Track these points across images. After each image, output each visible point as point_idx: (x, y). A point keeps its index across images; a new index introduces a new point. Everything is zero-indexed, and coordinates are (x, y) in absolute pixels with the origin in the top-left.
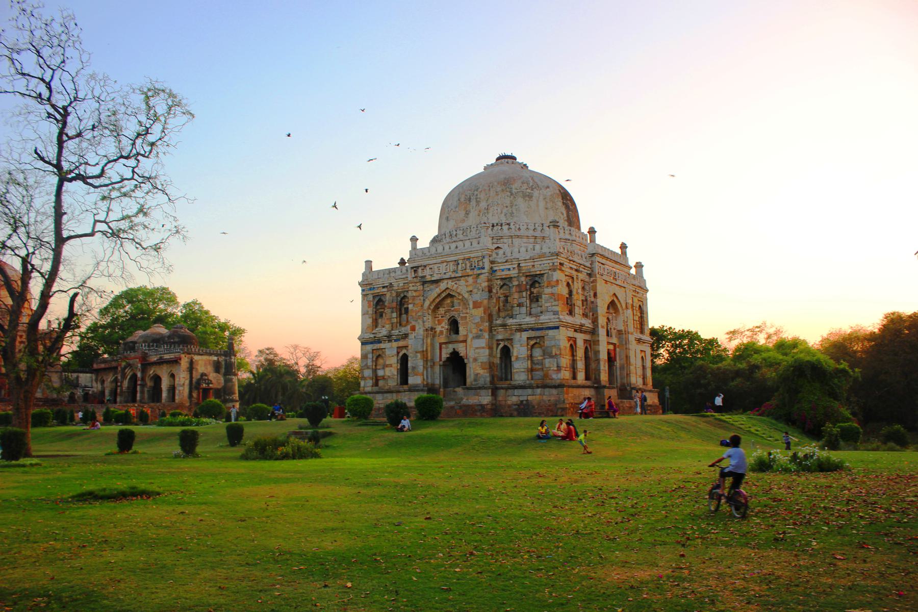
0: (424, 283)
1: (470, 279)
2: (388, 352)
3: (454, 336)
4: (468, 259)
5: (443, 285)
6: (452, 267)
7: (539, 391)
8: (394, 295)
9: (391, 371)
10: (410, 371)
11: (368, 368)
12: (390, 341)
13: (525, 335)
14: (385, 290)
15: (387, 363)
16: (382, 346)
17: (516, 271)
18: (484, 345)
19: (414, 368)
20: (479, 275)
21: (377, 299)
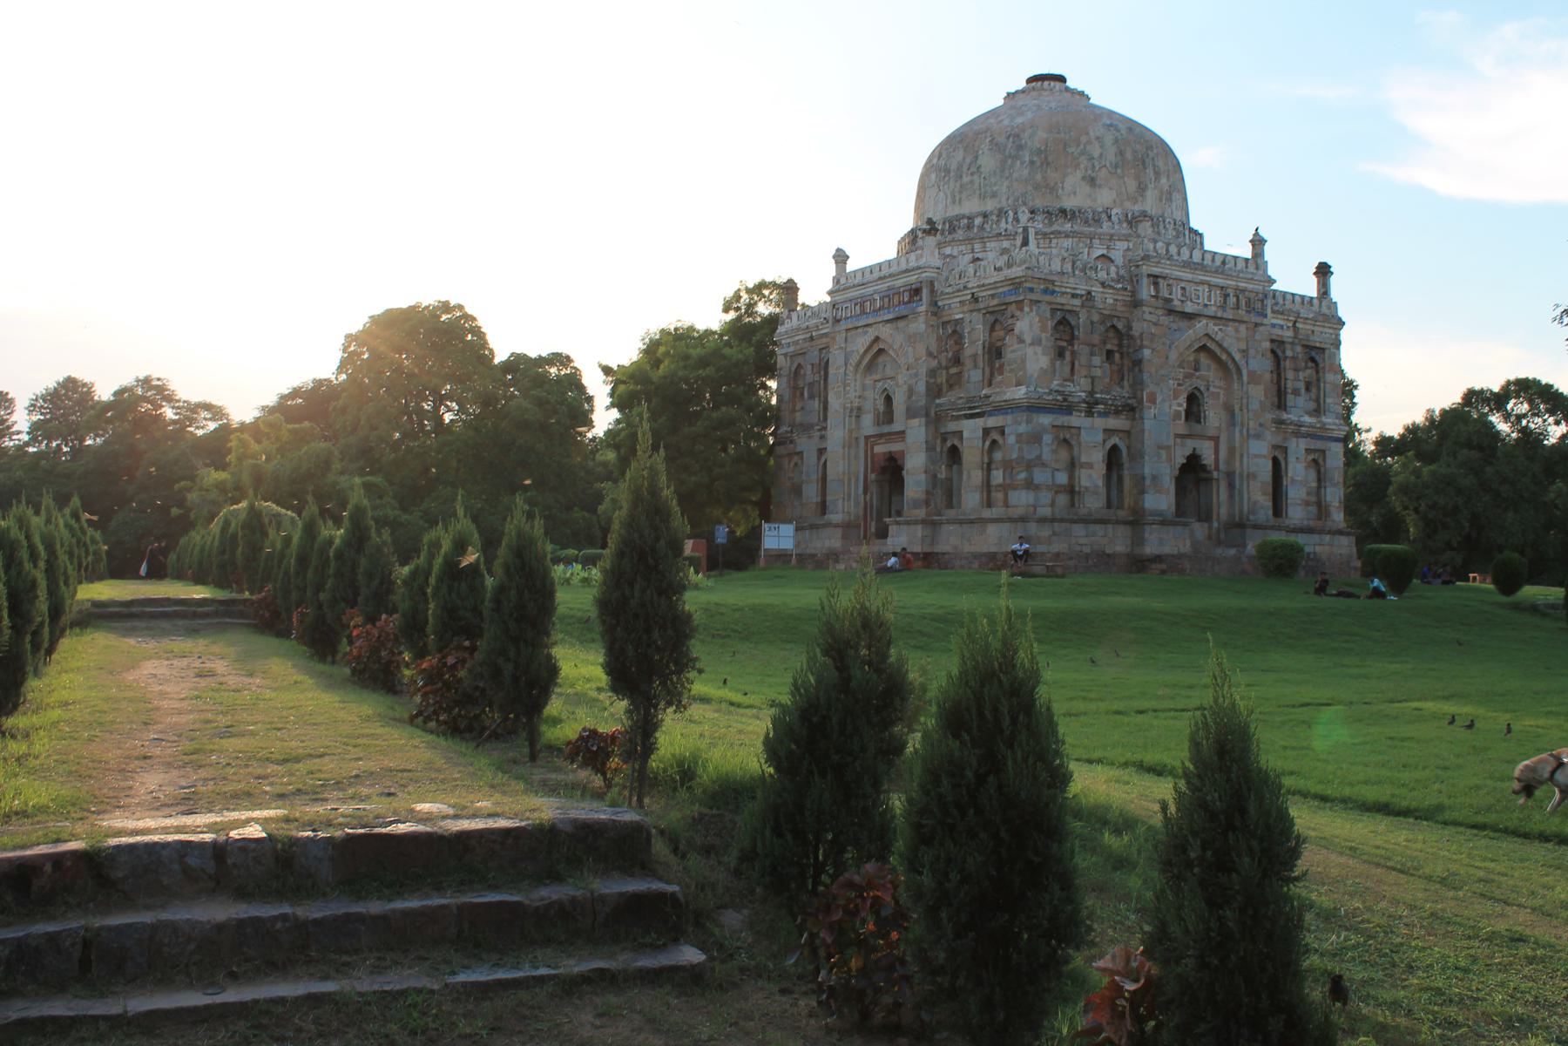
0: (1171, 312)
1: (1243, 328)
2: (1084, 436)
3: (1197, 428)
4: (1243, 291)
5: (1200, 326)
6: (1216, 296)
7: (1327, 538)
8: (1096, 318)
9: (1092, 477)
10: (1148, 482)
11: (1044, 465)
12: (1090, 413)
13: (1303, 444)
14: (1077, 302)
15: (1084, 459)
16: (1076, 420)
17: (1290, 333)
18: (1265, 451)
19: (1154, 478)
20: (1256, 325)
21: (1059, 315)
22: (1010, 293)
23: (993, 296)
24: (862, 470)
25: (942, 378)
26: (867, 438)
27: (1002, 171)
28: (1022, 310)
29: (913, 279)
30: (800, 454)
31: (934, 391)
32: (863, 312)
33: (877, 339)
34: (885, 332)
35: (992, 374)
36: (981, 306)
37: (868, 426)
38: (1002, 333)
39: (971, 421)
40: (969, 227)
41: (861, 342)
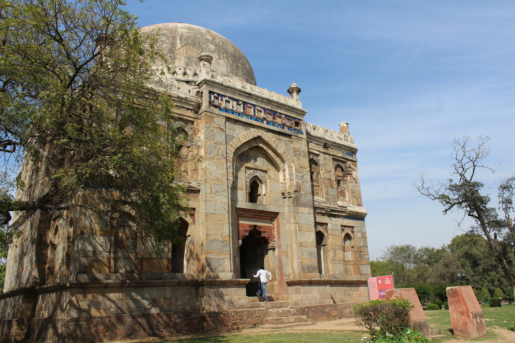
38: (340, 173)
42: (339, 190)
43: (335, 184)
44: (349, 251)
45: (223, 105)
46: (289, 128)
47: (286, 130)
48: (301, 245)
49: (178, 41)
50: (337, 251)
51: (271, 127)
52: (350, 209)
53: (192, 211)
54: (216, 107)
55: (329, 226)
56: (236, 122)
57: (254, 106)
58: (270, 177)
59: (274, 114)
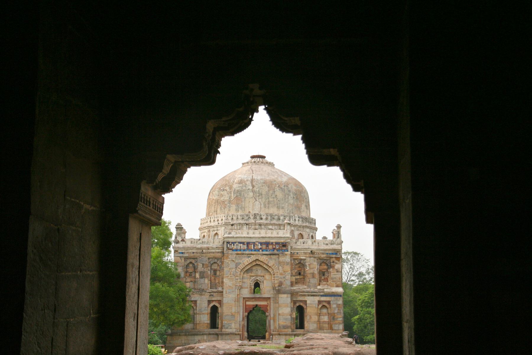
22: (332, 254)
23: (323, 253)
24: (242, 311)
25: (294, 278)
26: (244, 298)
27: (285, 199)
28: (339, 261)
29: (282, 241)
30: (195, 302)
31: (292, 285)
32: (248, 248)
33: (257, 260)
34: (263, 258)
35: (320, 281)
36: (316, 256)
37: (246, 293)
38: (326, 267)
39: (312, 297)
40: (279, 219)
41: (246, 261)
42: (323, 278)
43: (317, 276)
44: (326, 315)
45: (235, 247)
46: (278, 250)
47: (275, 252)
48: (279, 314)
49: (233, 195)
50: (312, 316)
51: (264, 253)
52: (325, 290)
53: (220, 302)
54: (230, 249)
55: (308, 302)
56: (243, 254)
57: (254, 243)
58: (266, 279)
59: (267, 244)
